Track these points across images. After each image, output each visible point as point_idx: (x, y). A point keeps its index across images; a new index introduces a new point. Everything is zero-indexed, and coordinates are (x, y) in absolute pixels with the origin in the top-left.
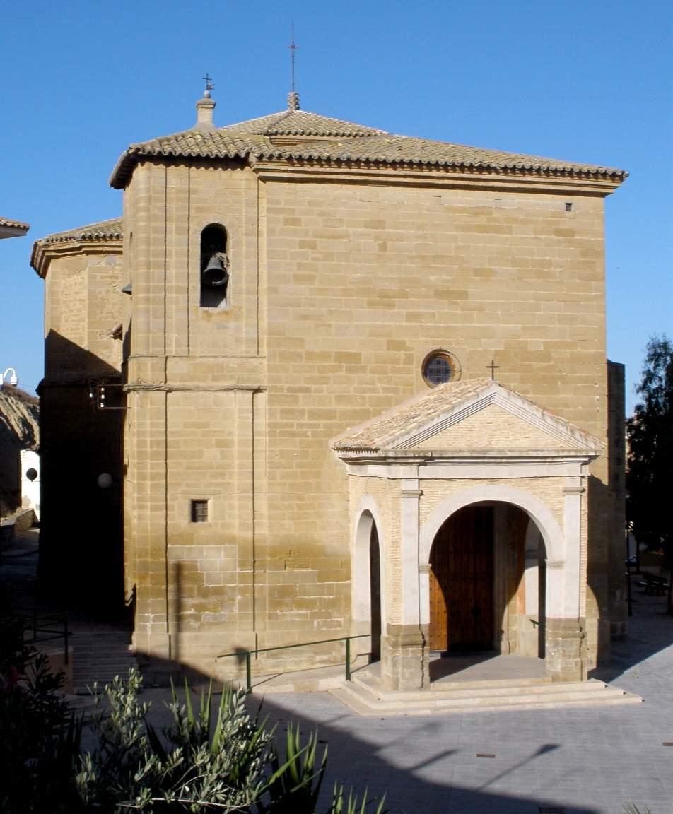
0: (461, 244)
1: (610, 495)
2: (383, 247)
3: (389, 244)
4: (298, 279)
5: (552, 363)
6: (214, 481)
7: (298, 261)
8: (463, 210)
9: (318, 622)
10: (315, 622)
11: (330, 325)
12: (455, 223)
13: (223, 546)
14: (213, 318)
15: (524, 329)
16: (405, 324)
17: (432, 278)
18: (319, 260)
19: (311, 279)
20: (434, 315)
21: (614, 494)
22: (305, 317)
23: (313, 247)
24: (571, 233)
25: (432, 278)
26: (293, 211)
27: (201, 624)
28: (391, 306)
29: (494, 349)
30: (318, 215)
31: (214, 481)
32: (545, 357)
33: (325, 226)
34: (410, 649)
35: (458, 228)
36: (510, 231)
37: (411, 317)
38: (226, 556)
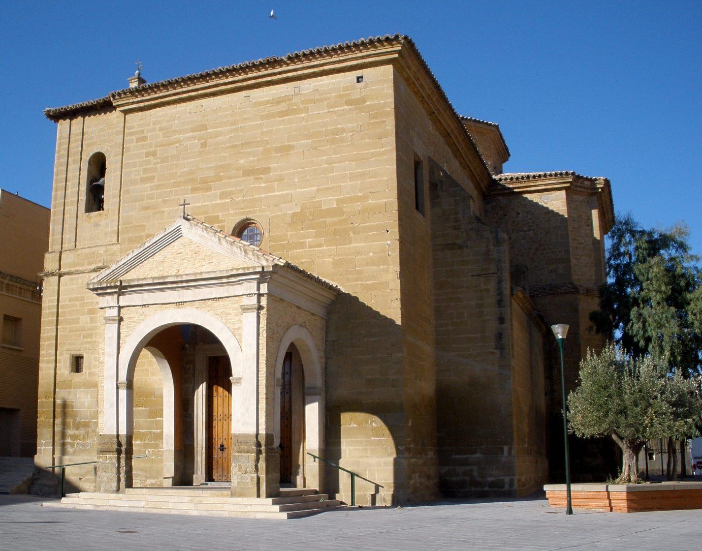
0: (265, 130)
1: (493, 353)
2: (204, 145)
3: (209, 141)
4: (144, 180)
5: (344, 217)
6: (86, 340)
7: (144, 167)
8: (268, 102)
9: (149, 452)
10: (147, 452)
11: (163, 212)
12: (260, 114)
13: (89, 390)
14: (92, 221)
15: (318, 190)
16: (219, 202)
17: (242, 161)
18: (158, 163)
19: (151, 179)
20: (241, 191)
21: (498, 352)
22: (147, 208)
23: (154, 154)
24: (363, 100)
25: (242, 161)
26: (143, 131)
27: (75, 450)
28: (208, 189)
29: (291, 212)
30: (159, 130)
31: (86, 340)
32: (338, 211)
33: (163, 137)
34: (108, 455)
35: (263, 118)
36: (306, 110)
37: (224, 195)
38: (91, 398)
